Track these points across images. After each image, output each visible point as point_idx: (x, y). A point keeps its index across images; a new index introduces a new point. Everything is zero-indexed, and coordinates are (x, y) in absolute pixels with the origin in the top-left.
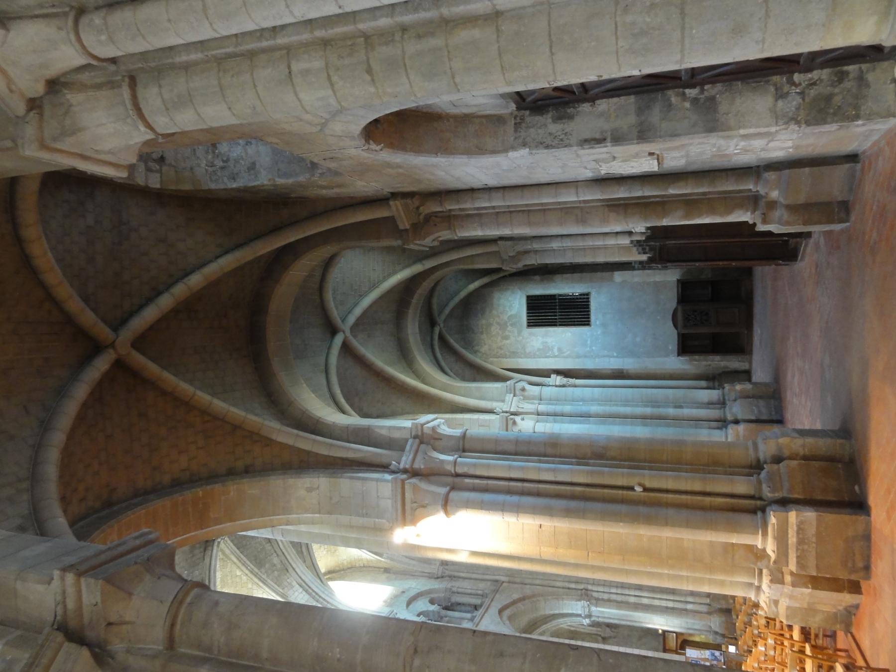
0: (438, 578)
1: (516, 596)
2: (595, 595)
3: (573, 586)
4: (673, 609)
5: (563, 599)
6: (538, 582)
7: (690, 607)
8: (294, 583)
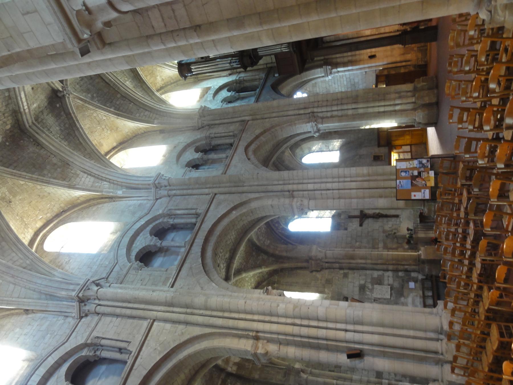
0: (199, 129)
1: (258, 132)
2: (320, 115)
3: (302, 112)
4: (384, 112)
5: (295, 124)
6: (274, 115)
7: (398, 108)
8: (79, 172)
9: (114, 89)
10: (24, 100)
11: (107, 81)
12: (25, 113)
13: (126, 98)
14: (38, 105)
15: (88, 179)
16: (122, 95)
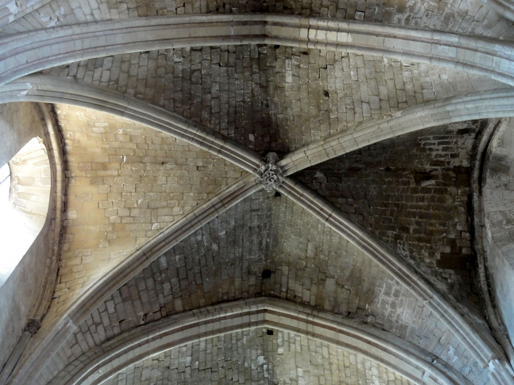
9: (199, 307)
10: (332, 36)
11: (224, 305)
12: (300, 27)
13: (162, 317)
14: (282, 89)
15: (87, 11)
16: (177, 313)
